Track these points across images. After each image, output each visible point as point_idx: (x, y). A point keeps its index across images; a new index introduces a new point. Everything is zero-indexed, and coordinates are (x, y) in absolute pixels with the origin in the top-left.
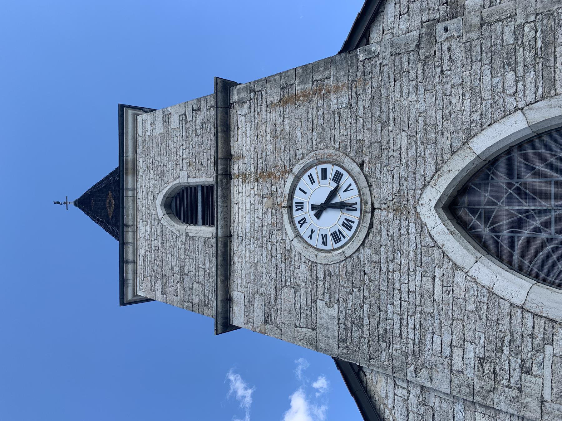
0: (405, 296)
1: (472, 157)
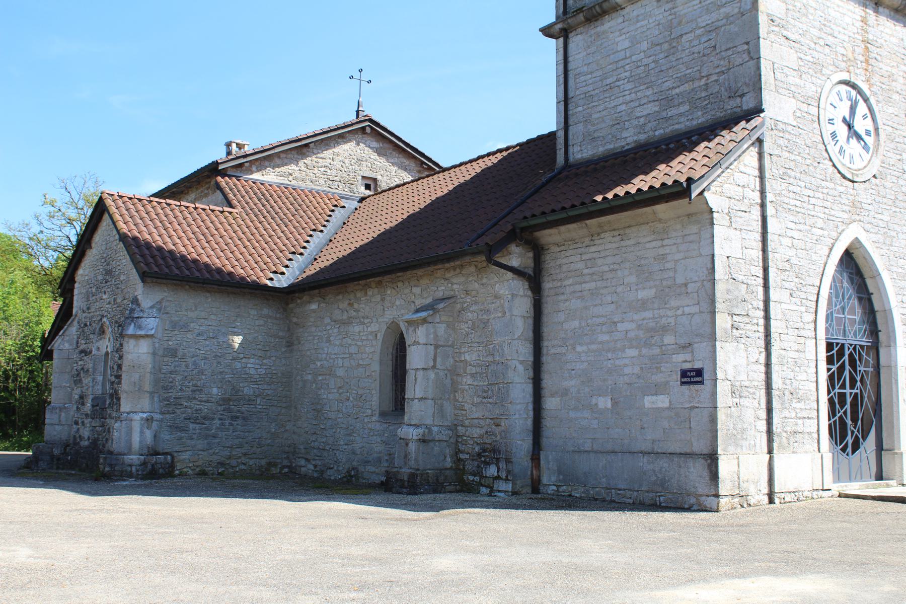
0: (813, 201)
1: (880, 270)
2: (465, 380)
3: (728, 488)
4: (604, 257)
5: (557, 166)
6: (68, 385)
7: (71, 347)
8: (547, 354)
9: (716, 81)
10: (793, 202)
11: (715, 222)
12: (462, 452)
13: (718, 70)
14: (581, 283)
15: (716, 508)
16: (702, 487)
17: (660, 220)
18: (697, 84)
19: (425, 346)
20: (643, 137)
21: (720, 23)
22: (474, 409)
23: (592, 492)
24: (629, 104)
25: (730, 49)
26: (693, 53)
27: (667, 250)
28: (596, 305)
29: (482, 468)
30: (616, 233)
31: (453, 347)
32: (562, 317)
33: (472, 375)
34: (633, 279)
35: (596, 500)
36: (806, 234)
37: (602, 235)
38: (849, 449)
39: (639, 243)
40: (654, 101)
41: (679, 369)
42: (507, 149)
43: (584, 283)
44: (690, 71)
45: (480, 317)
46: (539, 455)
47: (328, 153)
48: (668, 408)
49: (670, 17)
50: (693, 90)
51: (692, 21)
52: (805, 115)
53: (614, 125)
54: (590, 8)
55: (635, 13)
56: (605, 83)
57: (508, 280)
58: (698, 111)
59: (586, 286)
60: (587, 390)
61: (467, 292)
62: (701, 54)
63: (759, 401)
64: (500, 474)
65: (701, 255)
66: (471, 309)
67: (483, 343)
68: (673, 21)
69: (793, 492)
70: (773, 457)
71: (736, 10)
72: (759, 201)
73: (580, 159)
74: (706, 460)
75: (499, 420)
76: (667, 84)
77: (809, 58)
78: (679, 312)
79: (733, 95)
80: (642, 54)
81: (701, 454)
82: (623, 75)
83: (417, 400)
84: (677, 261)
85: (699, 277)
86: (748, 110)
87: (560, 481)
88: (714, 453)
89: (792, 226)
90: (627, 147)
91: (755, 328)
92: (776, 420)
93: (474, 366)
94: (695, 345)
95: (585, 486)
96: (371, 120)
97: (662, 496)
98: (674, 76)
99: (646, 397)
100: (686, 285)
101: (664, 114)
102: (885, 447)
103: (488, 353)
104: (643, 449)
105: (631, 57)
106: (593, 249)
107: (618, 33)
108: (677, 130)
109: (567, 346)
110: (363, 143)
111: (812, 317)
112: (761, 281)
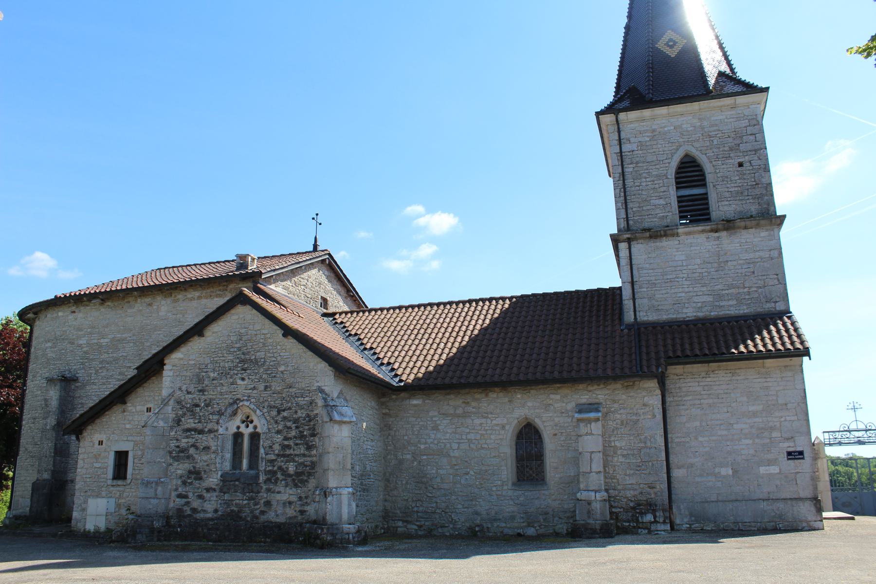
4: (719, 385)
6: (163, 460)
7: (166, 425)
8: (672, 442)
12: (615, 507)
15: (822, 528)
18: (741, 290)
21: (757, 260)
22: (627, 478)
25: (764, 275)
27: (770, 384)
28: (713, 413)
32: (684, 419)
33: (623, 456)
34: (745, 399)
35: (727, 530)
37: (717, 372)
45: (629, 418)
47: (305, 275)
49: (718, 249)
50: (739, 293)
53: (676, 304)
55: (689, 241)
56: (665, 277)
59: (706, 401)
60: (710, 464)
61: (614, 401)
64: (657, 519)
66: (619, 412)
67: (634, 434)
68: (721, 252)
71: (768, 256)
76: (719, 286)
82: (682, 276)
83: (594, 473)
84: (777, 391)
86: (780, 311)
87: (692, 521)
90: (687, 319)
95: (715, 522)
96: (329, 254)
99: (760, 467)
100: (786, 404)
101: (717, 304)
106: (708, 379)
107: (675, 250)
108: (728, 314)
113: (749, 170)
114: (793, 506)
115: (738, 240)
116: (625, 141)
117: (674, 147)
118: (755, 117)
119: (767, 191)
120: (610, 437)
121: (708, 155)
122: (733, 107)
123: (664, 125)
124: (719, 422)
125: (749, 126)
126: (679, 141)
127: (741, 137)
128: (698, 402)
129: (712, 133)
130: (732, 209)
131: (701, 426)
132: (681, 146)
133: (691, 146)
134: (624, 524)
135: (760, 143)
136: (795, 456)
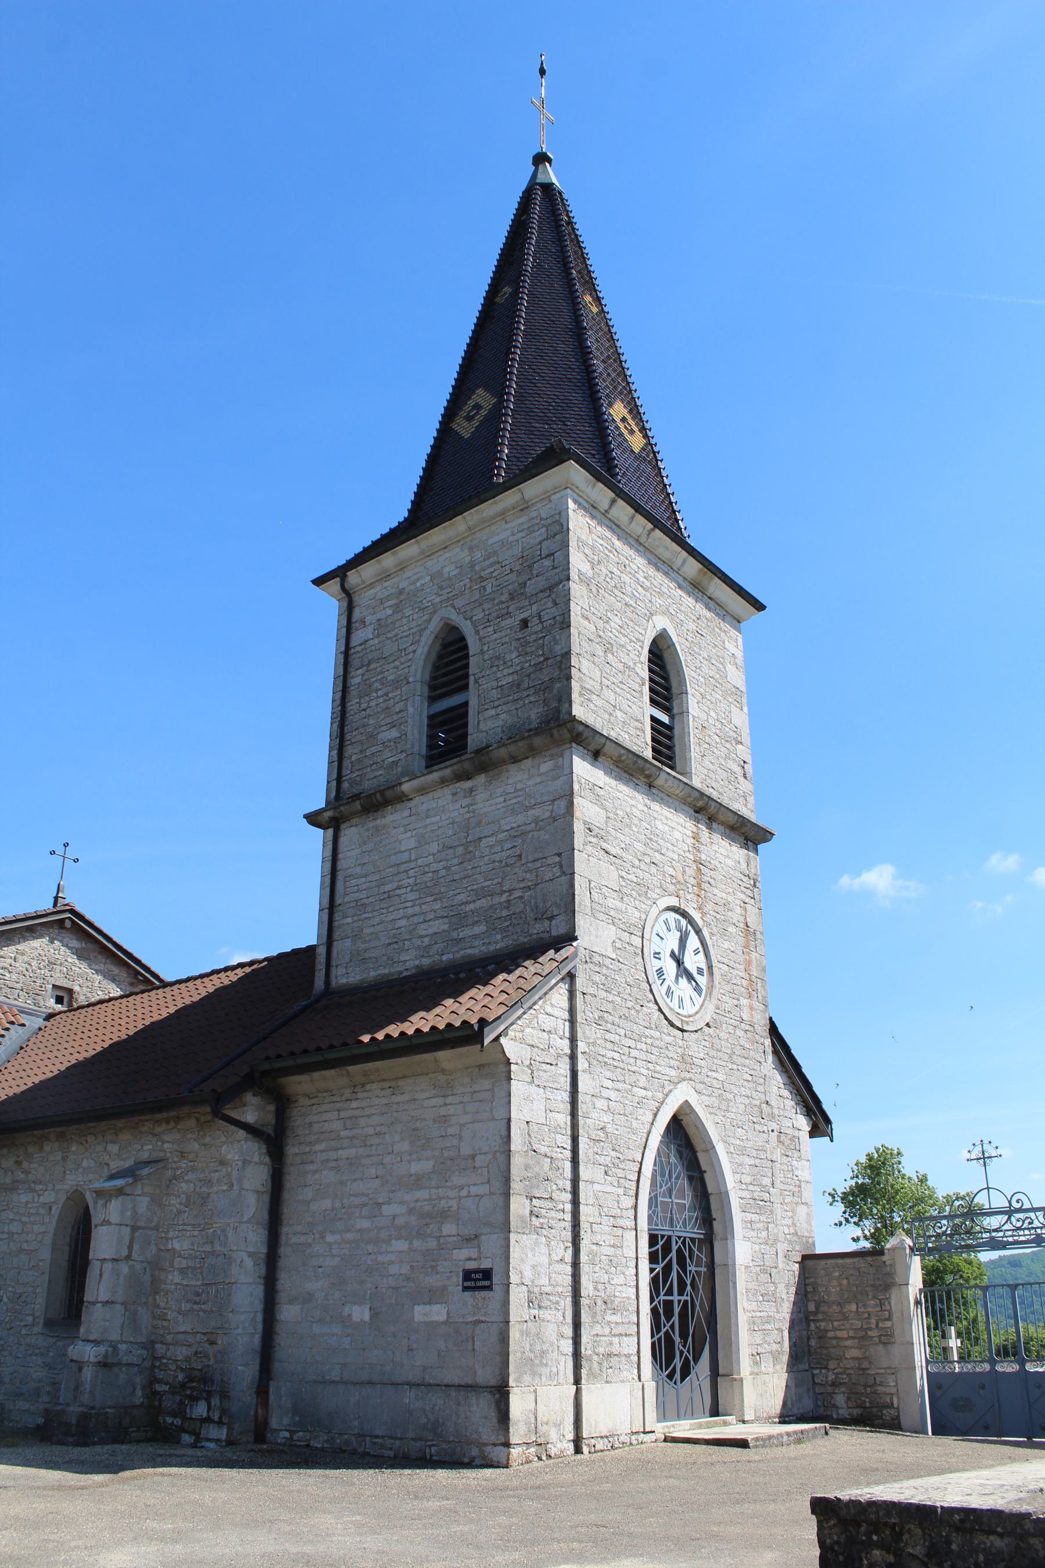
0: (634, 1053)
2: (170, 1277)
3: (522, 1433)
4: (369, 1116)
5: (314, 992)
9: (521, 898)
10: (610, 1054)
11: (512, 1077)
12: (159, 1381)
13: (522, 885)
14: (337, 1149)
15: (505, 1462)
16: (488, 1433)
17: (443, 1071)
18: (496, 900)
19: (118, 1227)
20: (426, 962)
22: (180, 1318)
23: (338, 1441)
24: (411, 919)
25: (538, 860)
26: (494, 861)
27: (451, 1110)
28: (355, 1180)
29: (186, 1406)
30: (386, 1085)
31: (158, 1230)
32: (309, 1193)
33: (182, 1271)
34: (405, 1146)
35: (345, 1452)
36: (625, 1095)
37: (368, 1087)
38: (678, 1376)
39: (415, 1100)
40: (443, 917)
41: (461, 1269)
42: (251, 963)
43: (341, 1149)
44: (488, 883)
45: (198, 1190)
46: (267, 1386)
48: (446, 1323)
49: (467, 816)
50: (491, 907)
51: (493, 822)
52: (627, 946)
54: (370, 796)
55: (425, 807)
56: (382, 890)
57: (239, 1141)
58: (497, 933)
59: (343, 1153)
60: (337, 1294)
61: (182, 1155)
62: (503, 864)
63: (564, 1314)
64: (211, 1414)
65: (494, 1119)
67: (199, 1225)
69: (607, 1437)
70: (581, 1388)
71: (547, 814)
72: (568, 1052)
73: (344, 985)
74: (494, 1395)
75: (214, 1335)
77: (632, 877)
78: (464, 1193)
79: (540, 916)
80: (431, 857)
81: (488, 1387)
82: (405, 882)
84: (462, 1126)
85: (490, 1147)
86: (558, 936)
88: (504, 1384)
89: (609, 1084)
90: (405, 974)
91: (560, 1215)
92: (584, 1339)
93: (184, 1258)
94: (483, 1238)
95: (330, 1432)
96: (73, 911)
97: (433, 1445)
98: (469, 889)
99: (416, 1307)
101: (454, 934)
102: (721, 1371)
103: (205, 1241)
104: (410, 1378)
105: (416, 860)
106: (354, 1104)
108: (470, 955)
109: (313, 1234)
110: (58, 940)
111: (629, 1202)
112: (568, 1154)
113: (536, 633)
114: (459, 1404)
115: (501, 790)
116: (357, 624)
117: (424, 618)
118: (557, 517)
119: (560, 668)
120: (168, 1232)
121: (474, 618)
122: (524, 507)
123: (416, 577)
124: (364, 1199)
125: (547, 539)
126: (434, 602)
127: (530, 567)
128: (332, 1155)
129: (486, 572)
130: (501, 723)
131: (332, 1209)
132: (435, 612)
133: (450, 608)
134: (167, 1418)
135: (561, 568)
136: (476, 1280)
